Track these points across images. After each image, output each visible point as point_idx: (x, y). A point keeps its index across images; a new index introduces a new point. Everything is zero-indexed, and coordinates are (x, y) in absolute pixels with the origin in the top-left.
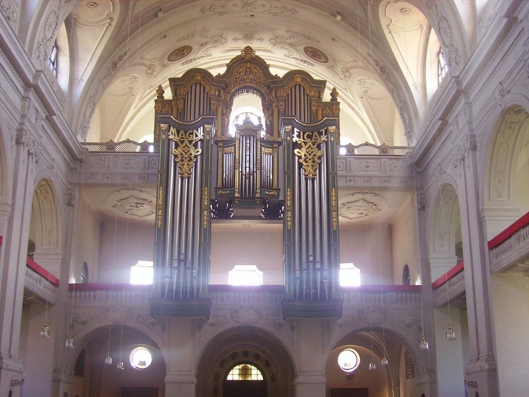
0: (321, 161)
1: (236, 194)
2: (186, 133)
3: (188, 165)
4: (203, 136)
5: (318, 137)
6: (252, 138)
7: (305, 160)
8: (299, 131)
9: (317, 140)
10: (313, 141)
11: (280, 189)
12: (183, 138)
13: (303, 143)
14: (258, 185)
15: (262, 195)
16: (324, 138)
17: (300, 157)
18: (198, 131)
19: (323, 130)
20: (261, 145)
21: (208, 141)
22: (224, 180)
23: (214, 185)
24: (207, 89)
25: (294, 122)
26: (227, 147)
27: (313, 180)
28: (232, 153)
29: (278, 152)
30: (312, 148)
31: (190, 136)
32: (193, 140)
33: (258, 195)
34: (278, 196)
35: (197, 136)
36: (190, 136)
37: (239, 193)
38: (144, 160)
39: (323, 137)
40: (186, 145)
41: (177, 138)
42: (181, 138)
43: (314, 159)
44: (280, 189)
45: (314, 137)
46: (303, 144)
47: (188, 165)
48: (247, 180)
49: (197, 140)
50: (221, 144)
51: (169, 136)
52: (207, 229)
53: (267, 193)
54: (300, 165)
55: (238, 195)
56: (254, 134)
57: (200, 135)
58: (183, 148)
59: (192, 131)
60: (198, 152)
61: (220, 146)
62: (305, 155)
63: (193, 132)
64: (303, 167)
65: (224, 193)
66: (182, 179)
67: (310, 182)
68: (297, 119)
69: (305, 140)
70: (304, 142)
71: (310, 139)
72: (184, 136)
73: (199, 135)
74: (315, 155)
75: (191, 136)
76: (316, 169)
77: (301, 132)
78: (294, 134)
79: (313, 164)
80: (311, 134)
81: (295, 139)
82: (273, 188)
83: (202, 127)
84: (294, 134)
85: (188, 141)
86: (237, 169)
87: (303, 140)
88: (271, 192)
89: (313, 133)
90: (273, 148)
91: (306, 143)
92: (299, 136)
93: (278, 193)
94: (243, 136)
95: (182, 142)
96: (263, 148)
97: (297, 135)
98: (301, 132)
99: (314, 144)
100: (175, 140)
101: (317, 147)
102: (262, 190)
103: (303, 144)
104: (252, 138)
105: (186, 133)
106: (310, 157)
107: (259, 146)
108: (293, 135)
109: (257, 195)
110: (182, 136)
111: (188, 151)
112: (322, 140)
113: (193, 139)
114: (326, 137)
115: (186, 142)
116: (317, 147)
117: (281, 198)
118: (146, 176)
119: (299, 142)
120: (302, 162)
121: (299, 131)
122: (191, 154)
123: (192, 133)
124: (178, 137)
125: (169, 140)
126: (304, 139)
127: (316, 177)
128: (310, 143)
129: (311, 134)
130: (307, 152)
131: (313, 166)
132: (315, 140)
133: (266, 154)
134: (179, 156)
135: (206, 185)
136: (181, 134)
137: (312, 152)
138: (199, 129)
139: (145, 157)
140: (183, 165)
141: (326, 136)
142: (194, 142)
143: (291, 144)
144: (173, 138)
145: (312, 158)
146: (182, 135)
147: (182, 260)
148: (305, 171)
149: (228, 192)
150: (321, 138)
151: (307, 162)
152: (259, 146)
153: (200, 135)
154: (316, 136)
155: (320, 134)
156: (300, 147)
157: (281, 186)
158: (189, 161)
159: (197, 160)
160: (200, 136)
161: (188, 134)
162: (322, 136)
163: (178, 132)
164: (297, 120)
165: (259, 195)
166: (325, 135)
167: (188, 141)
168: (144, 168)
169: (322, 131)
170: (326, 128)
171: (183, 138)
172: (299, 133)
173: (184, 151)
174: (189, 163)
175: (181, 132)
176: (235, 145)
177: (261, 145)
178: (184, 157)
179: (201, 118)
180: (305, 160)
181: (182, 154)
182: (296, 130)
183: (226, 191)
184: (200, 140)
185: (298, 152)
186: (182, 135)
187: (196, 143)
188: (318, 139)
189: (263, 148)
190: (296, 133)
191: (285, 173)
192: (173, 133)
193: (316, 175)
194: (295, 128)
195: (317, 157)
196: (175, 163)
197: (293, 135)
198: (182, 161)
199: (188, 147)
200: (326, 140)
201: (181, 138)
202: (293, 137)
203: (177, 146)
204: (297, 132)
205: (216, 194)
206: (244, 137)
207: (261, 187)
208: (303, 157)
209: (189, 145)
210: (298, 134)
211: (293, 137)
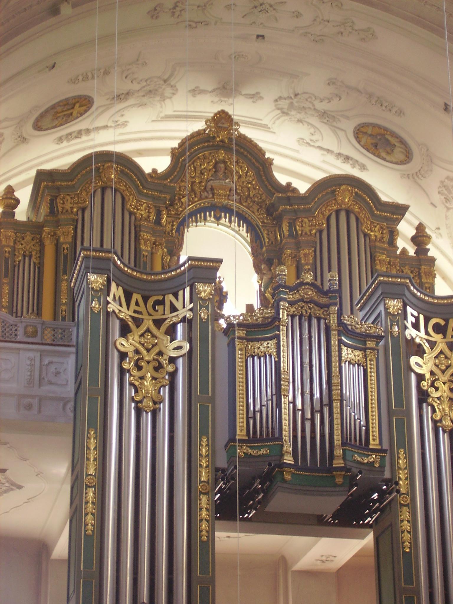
2: (146, 299)
4: (191, 310)
6: (315, 322)
12: (140, 313)
13: (427, 344)
17: (420, 378)
23: (222, 437)
32: (166, 319)
35: (174, 309)
38: (28, 362)
42: (135, 312)
48: (308, 425)
49: (175, 320)
53: (357, 457)
54: (423, 396)
57: (184, 307)
59: (161, 298)
62: (432, 373)
63: (164, 299)
64: (430, 400)
65: (254, 452)
70: (428, 341)
72: (142, 308)
73: (178, 305)
75: (159, 308)
77: (422, 317)
80: (442, 323)
83: (187, 290)
87: (426, 337)
88: (368, 456)
90: (364, 350)
91: (432, 344)
92: (416, 326)
94: (293, 317)
95: (138, 322)
96: (344, 349)
97: (412, 323)
102: (347, 451)
104: (315, 322)
105: (146, 299)
110: (137, 308)
113: (164, 317)
118: (35, 402)
119: (418, 340)
121: (416, 314)
122: (160, 353)
123: (162, 303)
124: (128, 310)
125: (108, 313)
126: (427, 333)
129: (442, 323)
130: (437, 366)
135: (204, 432)
136: (133, 302)
138: (181, 293)
139: (31, 354)
140: (142, 378)
143: (402, 343)
146: (137, 304)
149: (262, 451)
153: (184, 307)
156: (420, 351)
160: (184, 312)
161: (151, 302)
165: (342, 461)
168: (30, 382)
171: (140, 313)
172: (417, 319)
173: (143, 345)
175: (136, 297)
176: (278, 337)
177: (340, 342)
180: (432, 385)
181: (137, 352)
182: (409, 310)
183: (259, 448)
184: (184, 320)
186: (137, 304)
187: (174, 326)
189: (344, 349)
190: (411, 319)
194: (408, 307)
199: (153, 336)
201: (135, 312)
203: (125, 331)
204: (412, 315)
207: (344, 444)
208: (428, 376)
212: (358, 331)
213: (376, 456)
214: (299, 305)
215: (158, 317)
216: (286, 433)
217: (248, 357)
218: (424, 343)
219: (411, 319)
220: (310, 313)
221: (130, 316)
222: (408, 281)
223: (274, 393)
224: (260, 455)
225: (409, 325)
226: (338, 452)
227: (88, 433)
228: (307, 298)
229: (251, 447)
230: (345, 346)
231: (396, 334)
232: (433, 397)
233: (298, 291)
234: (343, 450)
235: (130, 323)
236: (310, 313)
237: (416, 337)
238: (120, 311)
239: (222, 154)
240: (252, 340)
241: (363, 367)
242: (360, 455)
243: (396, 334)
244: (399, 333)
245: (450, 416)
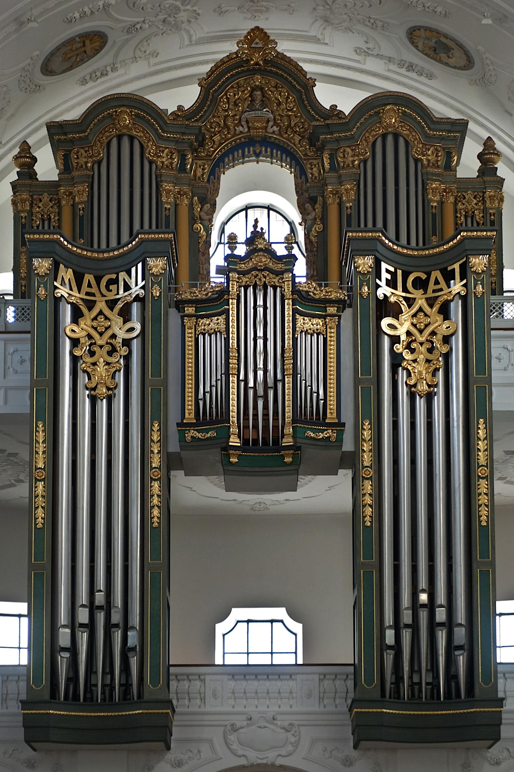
0: (451, 349)
1: (231, 440)
2: (98, 280)
3: (108, 364)
4: (143, 287)
5: (443, 284)
6: (270, 291)
7: (408, 347)
8: (392, 269)
9: (440, 293)
10: (430, 294)
11: (344, 423)
12: (93, 295)
13: (404, 302)
14: (289, 414)
15: (299, 440)
16: (457, 287)
17: (395, 340)
18: (130, 275)
19: (456, 267)
20: (293, 309)
21: (156, 301)
22: (201, 403)
24: (151, 149)
25: (380, 247)
26: (208, 316)
27: (429, 397)
28: (221, 333)
29: (338, 326)
30: (426, 315)
31: (111, 287)
33: (288, 441)
34: (340, 440)
35: (127, 288)
36: (111, 287)
37: (239, 437)
39: (455, 285)
40: (101, 313)
41: (77, 295)
42: (87, 294)
43: (432, 343)
44: (344, 423)
45: (431, 286)
46: (404, 306)
47: (108, 364)
49: (129, 299)
50: (190, 310)
51: (57, 291)
52: (160, 526)
55: (238, 441)
56: (276, 281)
57: (136, 285)
58: (93, 320)
59: (114, 276)
60: (132, 329)
61: (190, 316)
63: (117, 277)
64: (404, 364)
65: (199, 435)
66: (93, 400)
67: (421, 404)
68: (387, 238)
69: (409, 292)
70: (405, 298)
71: (421, 291)
72: (94, 290)
74: (433, 333)
75: (113, 287)
76: (437, 370)
77: (399, 272)
78: (380, 280)
79: (430, 357)
80: (424, 276)
81: (384, 291)
82: (327, 421)
84: (380, 280)
85: (106, 301)
86: (232, 374)
87: (404, 294)
88: (322, 431)
89: (429, 275)
90: (324, 317)
92: (392, 283)
93: (340, 434)
95: (90, 305)
98: (399, 272)
99: (431, 302)
100: (73, 300)
101: (440, 312)
102: (298, 429)
103: (404, 306)
104: (270, 291)
105: (98, 280)
106: (421, 339)
107: (289, 312)
108: (378, 281)
109: (284, 440)
110: (89, 290)
111: (107, 329)
112: (454, 293)
113: (118, 297)
114: (465, 285)
115: (101, 305)
116: (440, 312)
117: (348, 446)
119: (393, 299)
120: (400, 351)
122: (114, 336)
123: (115, 281)
124: (79, 293)
126: (405, 289)
127: (436, 389)
128: (421, 302)
130: (414, 326)
131: (428, 361)
132: (434, 291)
133: (306, 332)
134: (82, 341)
137: (426, 326)
138: (133, 270)
140: (94, 364)
141: (465, 281)
142: (120, 305)
143: (372, 305)
144: (66, 295)
145: (427, 340)
146: (89, 285)
147: (100, 608)
148: (409, 375)
150: (449, 287)
151: (413, 351)
152: (289, 312)
153: (136, 285)
154: (437, 282)
155: (449, 276)
157: (348, 417)
158: (110, 353)
159: (130, 352)
162: (452, 282)
163: (79, 279)
164: (387, 242)
165: (291, 440)
166: (462, 280)
167: (106, 301)
169: (454, 269)
170: (465, 259)
171: (93, 295)
172: (394, 275)
173: (95, 329)
174: (110, 359)
175: (89, 277)
177: (295, 312)
178: (95, 343)
179: (137, 240)
180: (408, 347)
181: (90, 336)
182: (384, 266)
183: (207, 431)
184: (137, 298)
185: (391, 326)
188: (441, 290)
191: (357, 382)
192: (67, 281)
193: (436, 386)
194: (382, 263)
195: (440, 337)
196: (75, 360)
197: (378, 281)
198: (92, 354)
200: (463, 293)
201: (87, 294)
202: (378, 286)
204: (387, 271)
205: (182, 439)
206: (250, 290)
207: (294, 421)
208: (403, 337)
209: (107, 312)
210: (389, 277)
211: (378, 286)
212: (317, 297)
213: (332, 430)
214: (253, 275)
215: (111, 296)
216: (234, 413)
217: (198, 335)
218: (400, 302)
219: (385, 276)
220: (265, 282)
221: (82, 299)
222: (381, 235)
223: (223, 372)
224: (208, 438)
225: (383, 283)
226: (288, 430)
227: (37, 426)
228: (260, 266)
229: (199, 431)
230: (301, 316)
231: (365, 295)
232: (408, 360)
233: (251, 259)
234: (293, 427)
235: (81, 306)
236: (265, 282)
237: (391, 296)
238: (69, 294)
239: (258, 80)
240: (202, 317)
241: (323, 335)
242: (314, 431)
243: (365, 295)
244: (369, 293)
245: (426, 380)
